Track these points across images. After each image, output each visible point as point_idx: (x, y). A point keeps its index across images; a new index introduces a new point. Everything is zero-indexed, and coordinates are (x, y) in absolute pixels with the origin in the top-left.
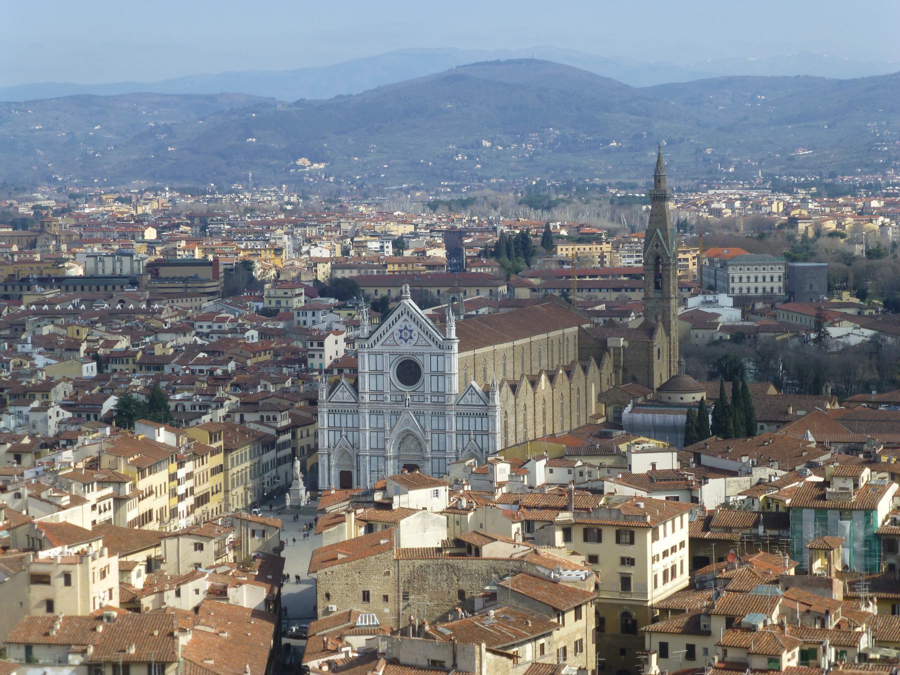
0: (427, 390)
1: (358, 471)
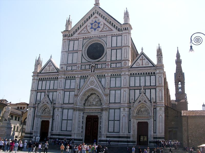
0: (108, 59)
1: (53, 120)
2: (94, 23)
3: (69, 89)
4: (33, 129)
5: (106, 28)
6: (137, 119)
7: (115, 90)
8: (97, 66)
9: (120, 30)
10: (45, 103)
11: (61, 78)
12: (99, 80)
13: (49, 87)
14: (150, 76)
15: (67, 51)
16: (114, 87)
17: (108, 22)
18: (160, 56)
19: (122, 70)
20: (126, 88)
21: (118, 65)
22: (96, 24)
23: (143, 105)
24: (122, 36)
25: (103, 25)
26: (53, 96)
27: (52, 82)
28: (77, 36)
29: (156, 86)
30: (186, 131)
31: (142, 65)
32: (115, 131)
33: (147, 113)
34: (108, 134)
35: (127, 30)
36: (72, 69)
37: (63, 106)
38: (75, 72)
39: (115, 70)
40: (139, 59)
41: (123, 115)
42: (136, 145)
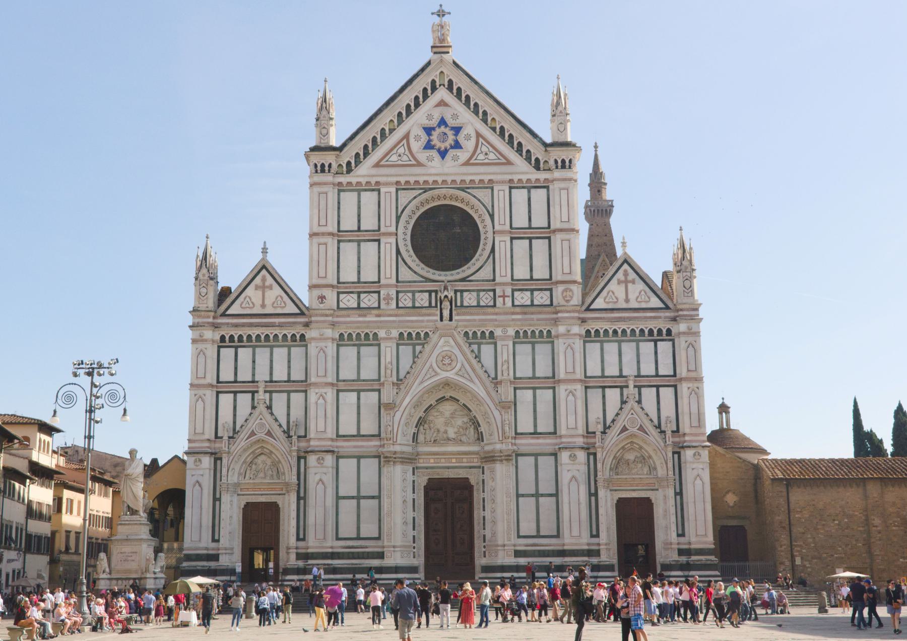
0: (503, 275)
1: (301, 498)
2: (439, 125)
3: (353, 381)
5: (486, 154)
6: (616, 490)
7: (534, 389)
8: (462, 296)
10: (261, 435)
11: (322, 338)
12: (472, 351)
13: (268, 373)
14: (656, 342)
15: (335, 231)
16: (530, 378)
17: (494, 129)
18: (688, 274)
19: (555, 316)
20: (575, 381)
21: (538, 298)
22: (447, 130)
24: (547, 188)
25: (473, 140)
26: (289, 407)
27: (280, 353)
28: (373, 176)
29: (675, 375)
30: (784, 528)
31: (627, 300)
32: (542, 534)
33: (646, 470)
34: (520, 545)
36: (359, 304)
37: (337, 447)
39: (532, 316)
40: (614, 280)
41: (569, 475)
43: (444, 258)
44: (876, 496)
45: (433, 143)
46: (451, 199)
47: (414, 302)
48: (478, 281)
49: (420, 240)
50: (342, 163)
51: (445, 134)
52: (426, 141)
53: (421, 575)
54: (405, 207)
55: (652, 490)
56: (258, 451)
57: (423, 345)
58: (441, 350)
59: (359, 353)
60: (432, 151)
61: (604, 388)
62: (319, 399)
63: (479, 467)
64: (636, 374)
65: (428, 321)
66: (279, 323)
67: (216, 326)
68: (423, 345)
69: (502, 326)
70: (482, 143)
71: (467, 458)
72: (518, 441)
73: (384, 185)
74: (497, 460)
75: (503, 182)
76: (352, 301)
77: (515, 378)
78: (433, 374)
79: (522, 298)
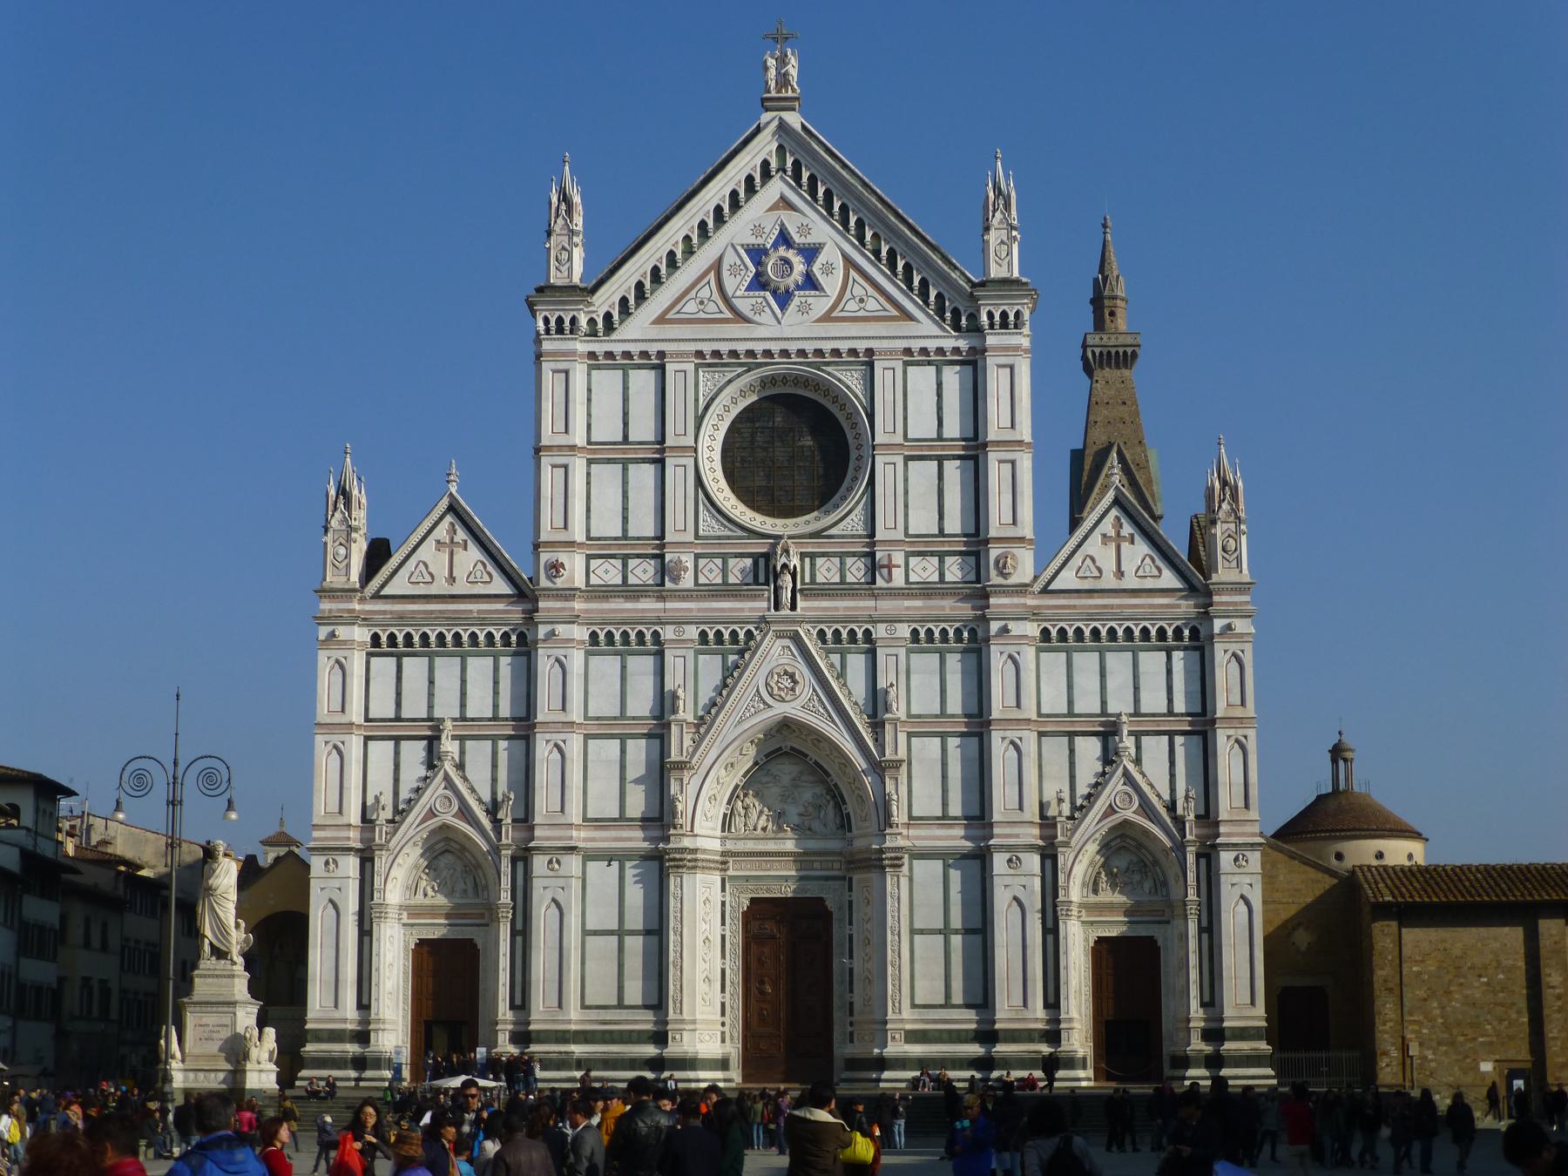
1: (522, 932)
2: (775, 246)
3: (615, 718)
4: (363, 1005)
5: (862, 301)
6: (1092, 923)
8: (813, 565)
9: (964, 321)
12: (832, 665)
19: (982, 602)
22: (790, 254)
23: (1119, 833)
24: (974, 364)
27: (480, 667)
31: (1120, 573)
33: (1148, 885)
35: (1016, 327)
36: (625, 578)
37: (585, 840)
38: (660, 605)
40: (1096, 537)
42: (1088, 1079)
43: (782, 493)
44: (1555, 932)
45: (763, 280)
46: (795, 385)
47: (725, 576)
48: (843, 537)
49: (739, 459)
50: (594, 316)
51: (786, 261)
52: (751, 275)
53: (736, 1075)
54: (712, 399)
55: (1159, 922)
56: (440, 845)
57: (741, 653)
58: (774, 664)
59: (624, 668)
60: (762, 293)
61: (1071, 735)
62: (551, 752)
63: (844, 878)
64: (1132, 712)
65: (751, 609)
66: (479, 612)
67: (366, 620)
68: (741, 653)
69: (887, 621)
70: (854, 280)
71: (821, 862)
72: (912, 832)
73: (672, 357)
74: (876, 867)
75: (891, 352)
76: (613, 572)
77: (909, 715)
78: (762, 705)
79: (924, 569)
